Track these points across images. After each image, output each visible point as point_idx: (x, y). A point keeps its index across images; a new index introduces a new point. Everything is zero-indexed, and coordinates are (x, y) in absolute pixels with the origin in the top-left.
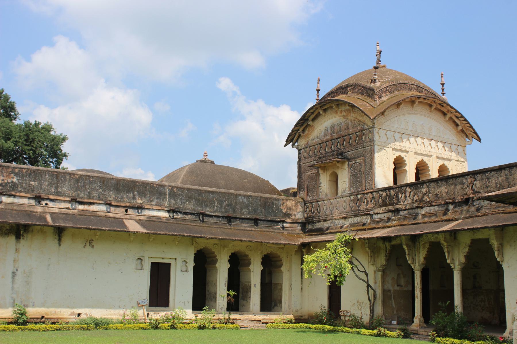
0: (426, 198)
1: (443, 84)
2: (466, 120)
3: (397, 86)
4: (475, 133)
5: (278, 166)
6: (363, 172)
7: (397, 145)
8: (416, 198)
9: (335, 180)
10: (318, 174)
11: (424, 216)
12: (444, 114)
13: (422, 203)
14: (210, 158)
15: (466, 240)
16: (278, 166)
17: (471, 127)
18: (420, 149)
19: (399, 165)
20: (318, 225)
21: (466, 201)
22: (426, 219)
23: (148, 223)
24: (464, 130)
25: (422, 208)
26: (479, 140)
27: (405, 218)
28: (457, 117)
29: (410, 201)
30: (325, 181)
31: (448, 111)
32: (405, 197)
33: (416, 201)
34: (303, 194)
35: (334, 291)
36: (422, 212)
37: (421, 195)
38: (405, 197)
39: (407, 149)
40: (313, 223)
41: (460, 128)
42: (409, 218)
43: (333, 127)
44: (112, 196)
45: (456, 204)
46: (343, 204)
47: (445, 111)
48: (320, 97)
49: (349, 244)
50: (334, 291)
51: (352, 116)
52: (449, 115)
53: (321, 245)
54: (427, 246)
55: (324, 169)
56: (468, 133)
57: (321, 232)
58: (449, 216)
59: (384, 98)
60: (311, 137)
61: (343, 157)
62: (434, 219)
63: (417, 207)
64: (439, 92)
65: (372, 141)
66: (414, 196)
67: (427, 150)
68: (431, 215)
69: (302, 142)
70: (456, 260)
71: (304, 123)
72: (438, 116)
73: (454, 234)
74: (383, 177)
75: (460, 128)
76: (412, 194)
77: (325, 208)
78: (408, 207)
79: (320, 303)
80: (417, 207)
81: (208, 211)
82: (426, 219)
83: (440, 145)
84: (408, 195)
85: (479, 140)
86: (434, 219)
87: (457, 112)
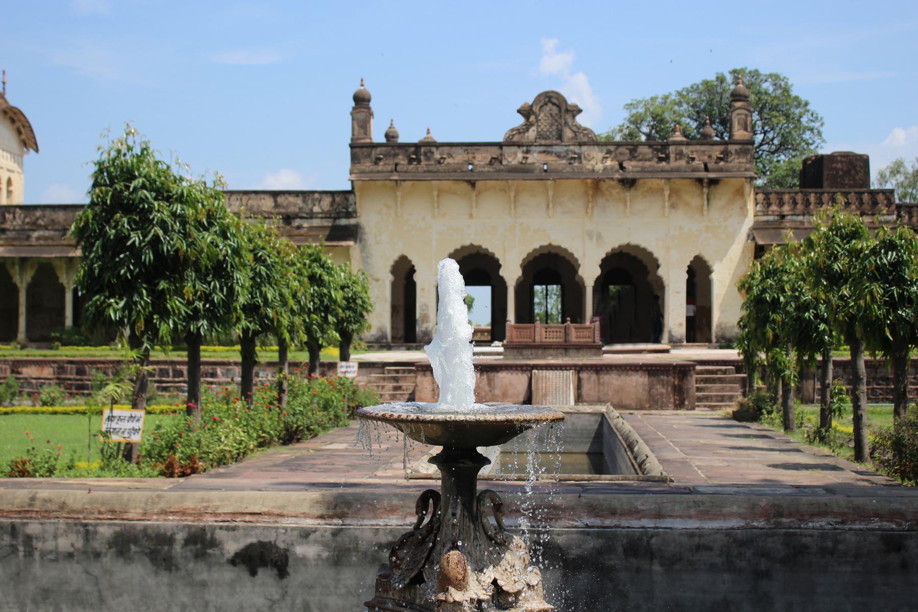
0: (41, 222)
1: (4, 83)
2: (32, 131)
4: (36, 144)
8: (27, 220)
11: (38, 239)
12: (13, 121)
13: (35, 226)
17: (34, 138)
22: (42, 242)
25: (34, 230)
26: (37, 150)
27: (14, 239)
28: (24, 126)
29: (20, 222)
31: (19, 120)
32: (14, 218)
33: (28, 223)
36: (35, 234)
37: (34, 219)
38: (14, 218)
41: (23, 137)
42: (19, 239)
47: (15, 118)
52: (18, 124)
54: (36, 266)
56: (27, 142)
62: (50, 242)
63: (30, 230)
66: (25, 217)
68: (46, 238)
72: (8, 123)
75: (23, 137)
76: (23, 216)
78: (17, 228)
80: (30, 230)
82: (42, 242)
83: (9, 155)
84: (17, 216)
85: (37, 150)
86: (50, 242)
87: (28, 122)
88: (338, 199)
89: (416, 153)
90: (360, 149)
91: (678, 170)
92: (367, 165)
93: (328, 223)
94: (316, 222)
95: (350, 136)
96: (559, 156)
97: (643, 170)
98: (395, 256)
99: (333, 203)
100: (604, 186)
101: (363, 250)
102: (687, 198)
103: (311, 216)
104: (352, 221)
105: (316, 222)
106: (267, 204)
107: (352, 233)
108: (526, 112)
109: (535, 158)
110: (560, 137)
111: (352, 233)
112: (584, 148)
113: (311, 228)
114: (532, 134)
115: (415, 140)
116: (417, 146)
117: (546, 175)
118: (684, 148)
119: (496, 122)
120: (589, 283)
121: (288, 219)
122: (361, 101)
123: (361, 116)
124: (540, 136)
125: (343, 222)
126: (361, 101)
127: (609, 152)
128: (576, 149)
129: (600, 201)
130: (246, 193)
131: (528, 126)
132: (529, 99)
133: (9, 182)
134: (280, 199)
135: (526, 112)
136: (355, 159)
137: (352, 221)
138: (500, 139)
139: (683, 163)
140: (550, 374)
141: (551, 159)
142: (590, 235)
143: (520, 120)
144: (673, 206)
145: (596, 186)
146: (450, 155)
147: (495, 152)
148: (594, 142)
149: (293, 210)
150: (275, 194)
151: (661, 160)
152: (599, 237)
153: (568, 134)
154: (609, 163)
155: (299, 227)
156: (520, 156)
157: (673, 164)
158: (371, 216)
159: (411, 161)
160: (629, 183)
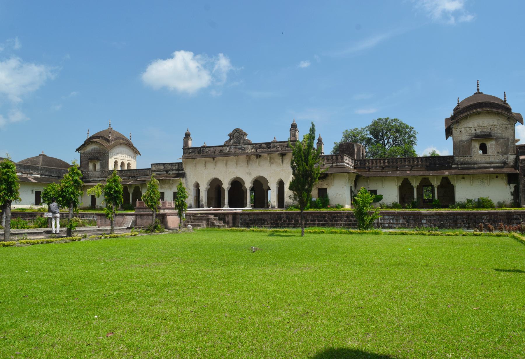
3: (117, 139)
5: (73, 158)
6: (105, 164)
7: (116, 157)
9: (95, 166)
10: (88, 163)
14: (44, 154)
15: (134, 186)
16: (73, 158)
18: (122, 158)
19: (116, 162)
20: (89, 179)
21: (134, 177)
23: (35, 178)
24: (136, 152)
30: (91, 166)
34: (82, 169)
35: (93, 199)
39: (119, 159)
40: (86, 178)
43: (94, 149)
44: (23, 170)
45: (132, 177)
46: (97, 174)
48: (89, 137)
49: (100, 186)
50: (93, 199)
51: (102, 147)
53: (92, 186)
55: (91, 162)
57: (89, 182)
58: (130, 180)
59: (113, 143)
60: (86, 150)
61: (98, 159)
64: (129, 139)
65: (108, 156)
67: (124, 158)
69: (82, 151)
70: (131, 191)
71: (83, 146)
73: (130, 185)
74: (111, 167)
77: (91, 174)
79: (89, 203)
81: (52, 175)
88: (180, 165)
89: (200, 150)
90: (186, 149)
91: (273, 151)
92: (187, 155)
93: (177, 172)
94: (174, 172)
95: (183, 146)
96: (239, 149)
97: (262, 152)
98: (194, 182)
99: (179, 166)
100: (252, 157)
101: (186, 180)
102: (276, 160)
103: (173, 170)
104: (183, 172)
105: (174, 172)
106: (162, 167)
107: (183, 175)
108: (230, 135)
109: (233, 150)
110: (239, 143)
111: (183, 175)
112: (246, 146)
113: (173, 174)
114: (231, 142)
115: (200, 146)
116: (200, 148)
117: (235, 154)
118: (275, 144)
119: (219, 138)
120: (248, 189)
121: (167, 171)
122: (187, 136)
123: (186, 140)
124: (234, 143)
125: (181, 172)
126: (187, 136)
127: (253, 147)
128: (244, 146)
129: (251, 162)
130: (157, 164)
131: (230, 140)
132: (231, 131)
133: (129, 164)
134: (165, 165)
135: (230, 135)
136: (184, 153)
137: (183, 172)
138: (223, 144)
139: (275, 149)
140: (128, 217)
141: (237, 150)
142: (247, 173)
143: (228, 138)
144: (272, 163)
145: (249, 157)
146: (209, 150)
147: (221, 148)
148: (250, 144)
149: (168, 169)
150: (164, 164)
151: (269, 148)
152: (250, 174)
153: (242, 141)
154: (253, 150)
155: (169, 174)
156: (228, 149)
157: (272, 149)
158: (188, 170)
159: (198, 153)
160: (259, 156)
